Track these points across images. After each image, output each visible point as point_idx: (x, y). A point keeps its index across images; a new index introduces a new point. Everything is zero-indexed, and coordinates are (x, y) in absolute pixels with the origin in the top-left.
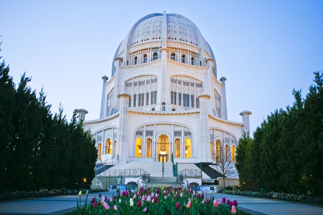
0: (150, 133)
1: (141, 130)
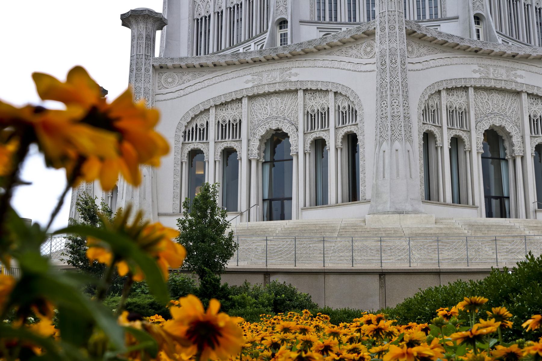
0: (230, 129)
1: (203, 123)
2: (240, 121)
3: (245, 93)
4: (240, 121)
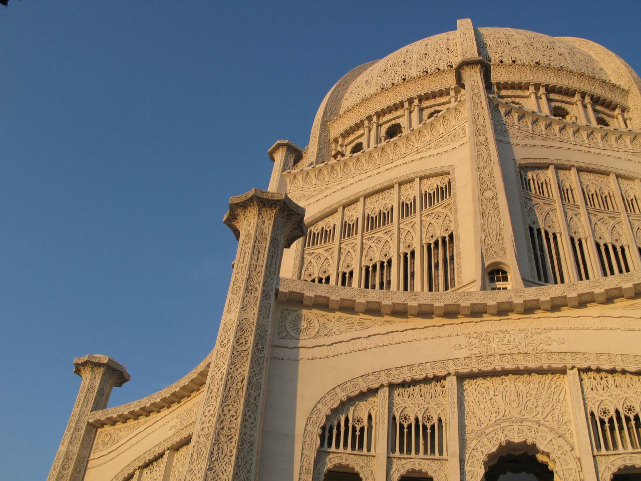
2: (440, 420)
3: (453, 369)
4: (440, 420)
